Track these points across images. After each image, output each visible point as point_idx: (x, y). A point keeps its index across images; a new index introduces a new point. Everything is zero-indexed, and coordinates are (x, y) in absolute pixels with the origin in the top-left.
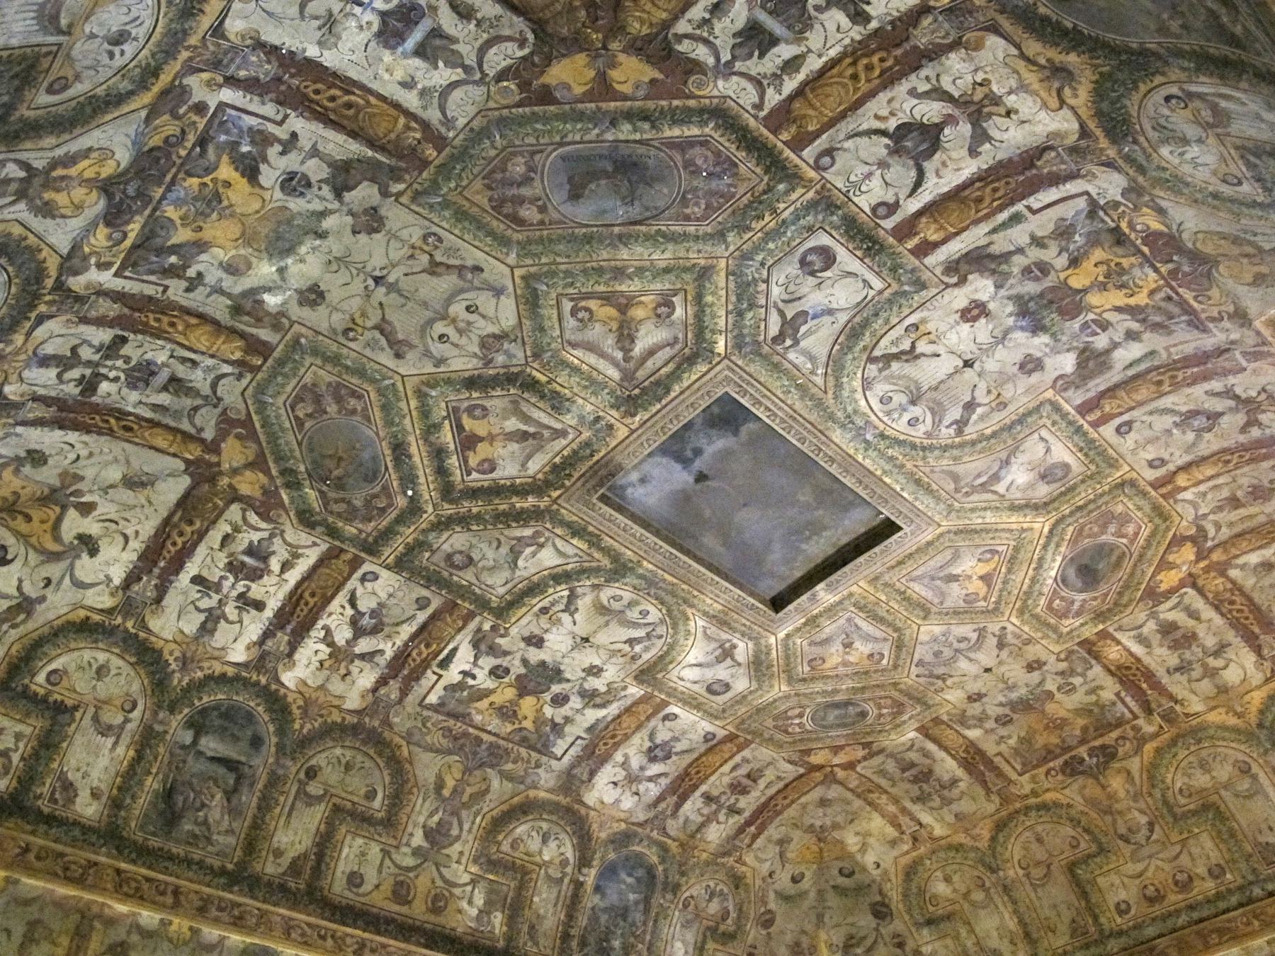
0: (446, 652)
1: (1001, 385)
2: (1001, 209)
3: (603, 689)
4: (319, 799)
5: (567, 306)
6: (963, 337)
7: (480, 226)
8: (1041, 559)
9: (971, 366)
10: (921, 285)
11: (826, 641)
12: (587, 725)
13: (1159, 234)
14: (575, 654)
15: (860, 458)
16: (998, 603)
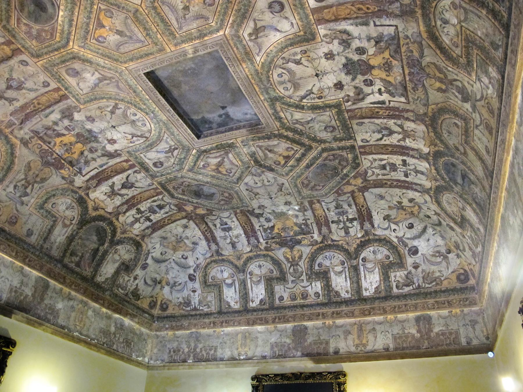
0: (376, 105)
2: (105, 169)
5: (231, 175)
6: (115, 135)
7: (239, 197)
8: (71, 26)
10: (128, 152)
12: (364, 28)
15: (157, 109)
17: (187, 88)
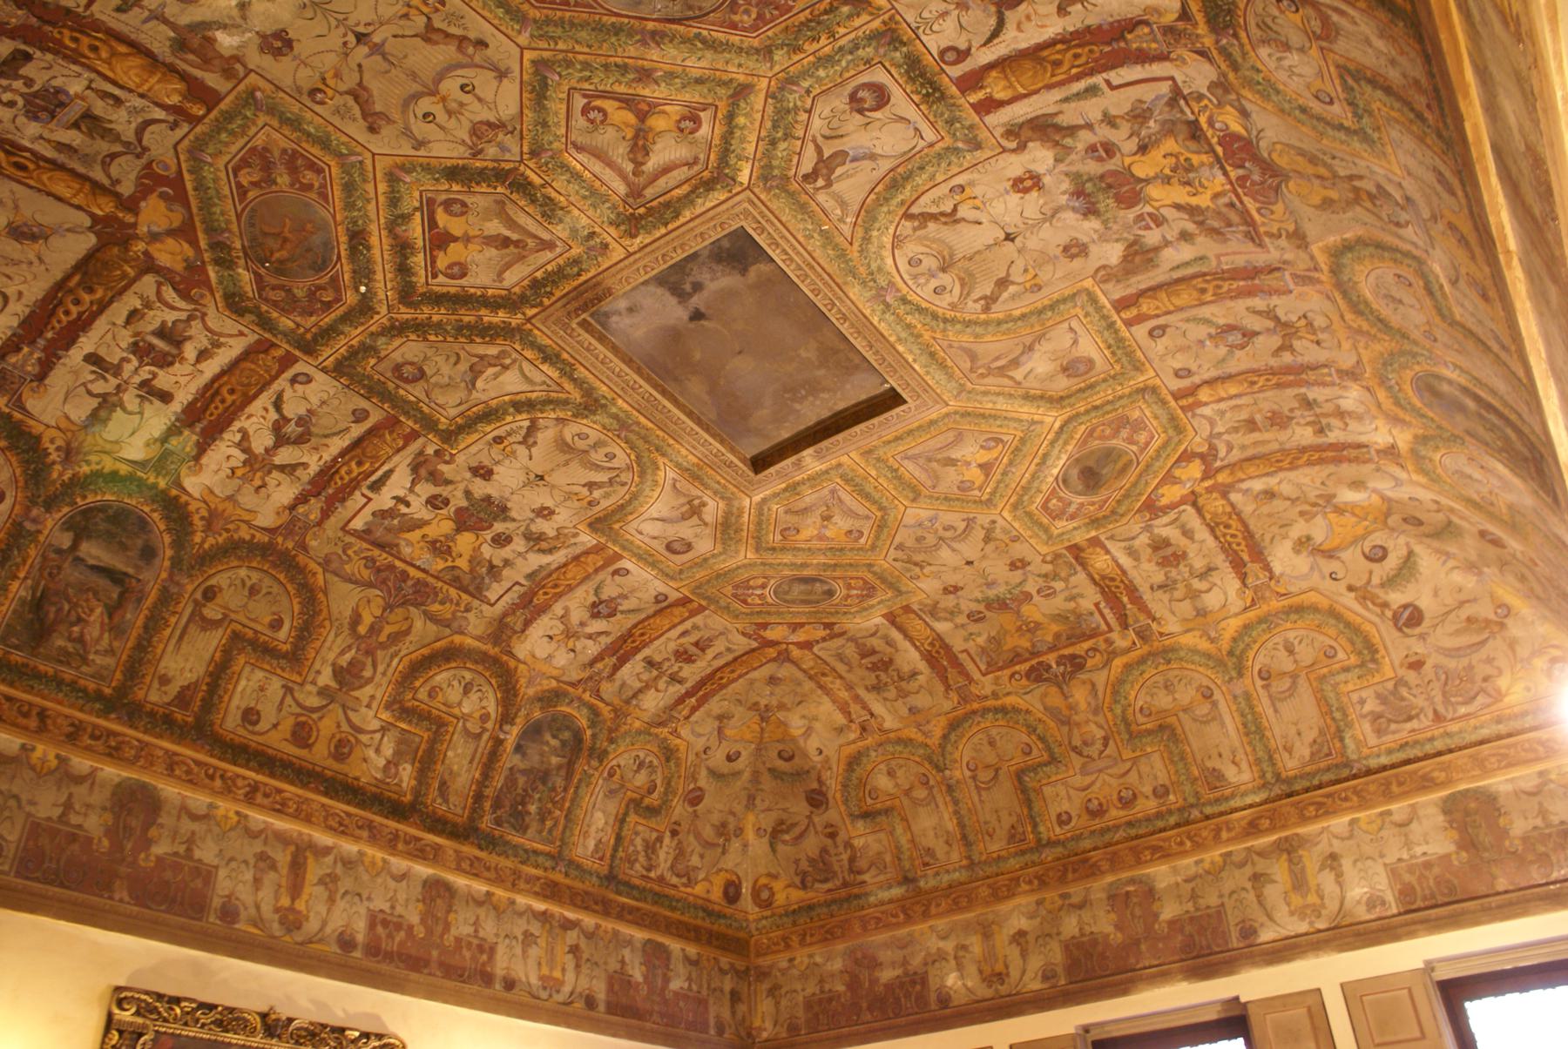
0: (380, 473)
1: (1040, 266)
2: (1078, 78)
3: (551, 533)
4: (215, 624)
5: (579, 102)
6: (1010, 208)
8: (1045, 456)
9: (1012, 240)
10: (978, 146)
11: (805, 511)
12: (529, 571)
13: (1236, 137)
14: (526, 492)
15: (875, 320)
16: (993, 493)
17: (803, 353)
